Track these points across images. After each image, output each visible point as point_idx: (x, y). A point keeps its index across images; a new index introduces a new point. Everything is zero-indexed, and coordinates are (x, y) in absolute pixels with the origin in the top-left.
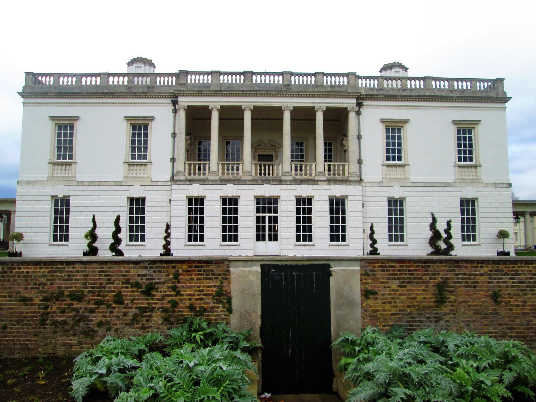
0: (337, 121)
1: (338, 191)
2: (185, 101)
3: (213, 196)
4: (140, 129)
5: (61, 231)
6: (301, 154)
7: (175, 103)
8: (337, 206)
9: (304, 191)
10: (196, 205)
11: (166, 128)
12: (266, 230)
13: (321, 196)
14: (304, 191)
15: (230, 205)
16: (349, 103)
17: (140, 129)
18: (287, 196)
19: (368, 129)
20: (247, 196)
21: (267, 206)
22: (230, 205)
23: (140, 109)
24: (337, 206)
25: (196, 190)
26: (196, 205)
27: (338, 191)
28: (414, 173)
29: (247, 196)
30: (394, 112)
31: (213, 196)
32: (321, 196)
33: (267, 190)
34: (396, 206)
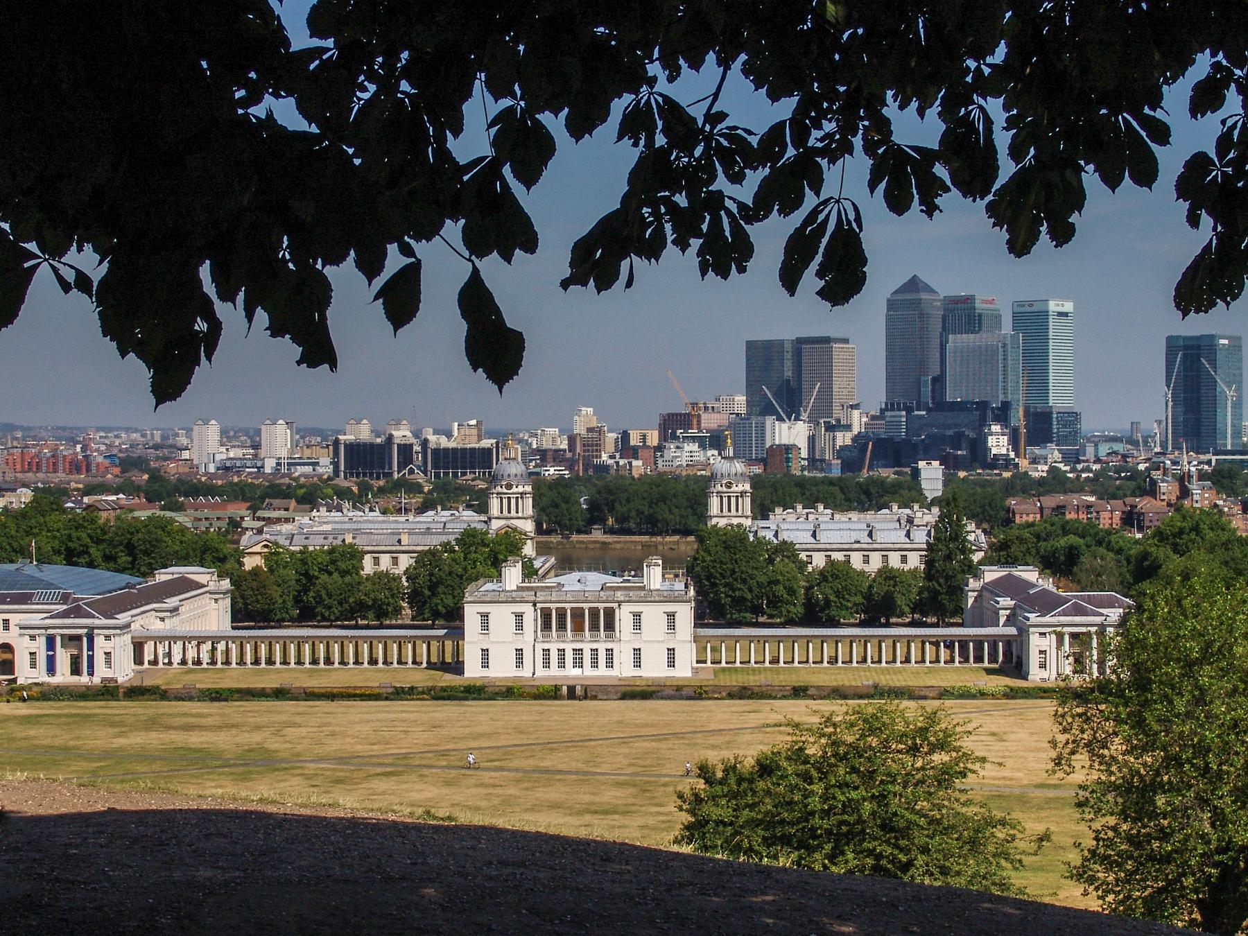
0: (610, 614)
1: (610, 646)
3: (554, 648)
4: (519, 616)
5: (485, 664)
6: (594, 627)
7: (535, 605)
8: (610, 652)
10: (546, 652)
12: (578, 663)
13: (602, 648)
15: (562, 652)
17: (519, 616)
18: (587, 648)
19: (624, 616)
20: (569, 648)
21: (578, 652)
22: (562, 652)
23: (518, 608)
24: (610, 652)
25: (546, 646)
26: (546, 652)
28: (645, 636)
29: (569, 648)
31: (554, 648)
32: (602, 648)
33: (578, 646)
34: (637, 651)
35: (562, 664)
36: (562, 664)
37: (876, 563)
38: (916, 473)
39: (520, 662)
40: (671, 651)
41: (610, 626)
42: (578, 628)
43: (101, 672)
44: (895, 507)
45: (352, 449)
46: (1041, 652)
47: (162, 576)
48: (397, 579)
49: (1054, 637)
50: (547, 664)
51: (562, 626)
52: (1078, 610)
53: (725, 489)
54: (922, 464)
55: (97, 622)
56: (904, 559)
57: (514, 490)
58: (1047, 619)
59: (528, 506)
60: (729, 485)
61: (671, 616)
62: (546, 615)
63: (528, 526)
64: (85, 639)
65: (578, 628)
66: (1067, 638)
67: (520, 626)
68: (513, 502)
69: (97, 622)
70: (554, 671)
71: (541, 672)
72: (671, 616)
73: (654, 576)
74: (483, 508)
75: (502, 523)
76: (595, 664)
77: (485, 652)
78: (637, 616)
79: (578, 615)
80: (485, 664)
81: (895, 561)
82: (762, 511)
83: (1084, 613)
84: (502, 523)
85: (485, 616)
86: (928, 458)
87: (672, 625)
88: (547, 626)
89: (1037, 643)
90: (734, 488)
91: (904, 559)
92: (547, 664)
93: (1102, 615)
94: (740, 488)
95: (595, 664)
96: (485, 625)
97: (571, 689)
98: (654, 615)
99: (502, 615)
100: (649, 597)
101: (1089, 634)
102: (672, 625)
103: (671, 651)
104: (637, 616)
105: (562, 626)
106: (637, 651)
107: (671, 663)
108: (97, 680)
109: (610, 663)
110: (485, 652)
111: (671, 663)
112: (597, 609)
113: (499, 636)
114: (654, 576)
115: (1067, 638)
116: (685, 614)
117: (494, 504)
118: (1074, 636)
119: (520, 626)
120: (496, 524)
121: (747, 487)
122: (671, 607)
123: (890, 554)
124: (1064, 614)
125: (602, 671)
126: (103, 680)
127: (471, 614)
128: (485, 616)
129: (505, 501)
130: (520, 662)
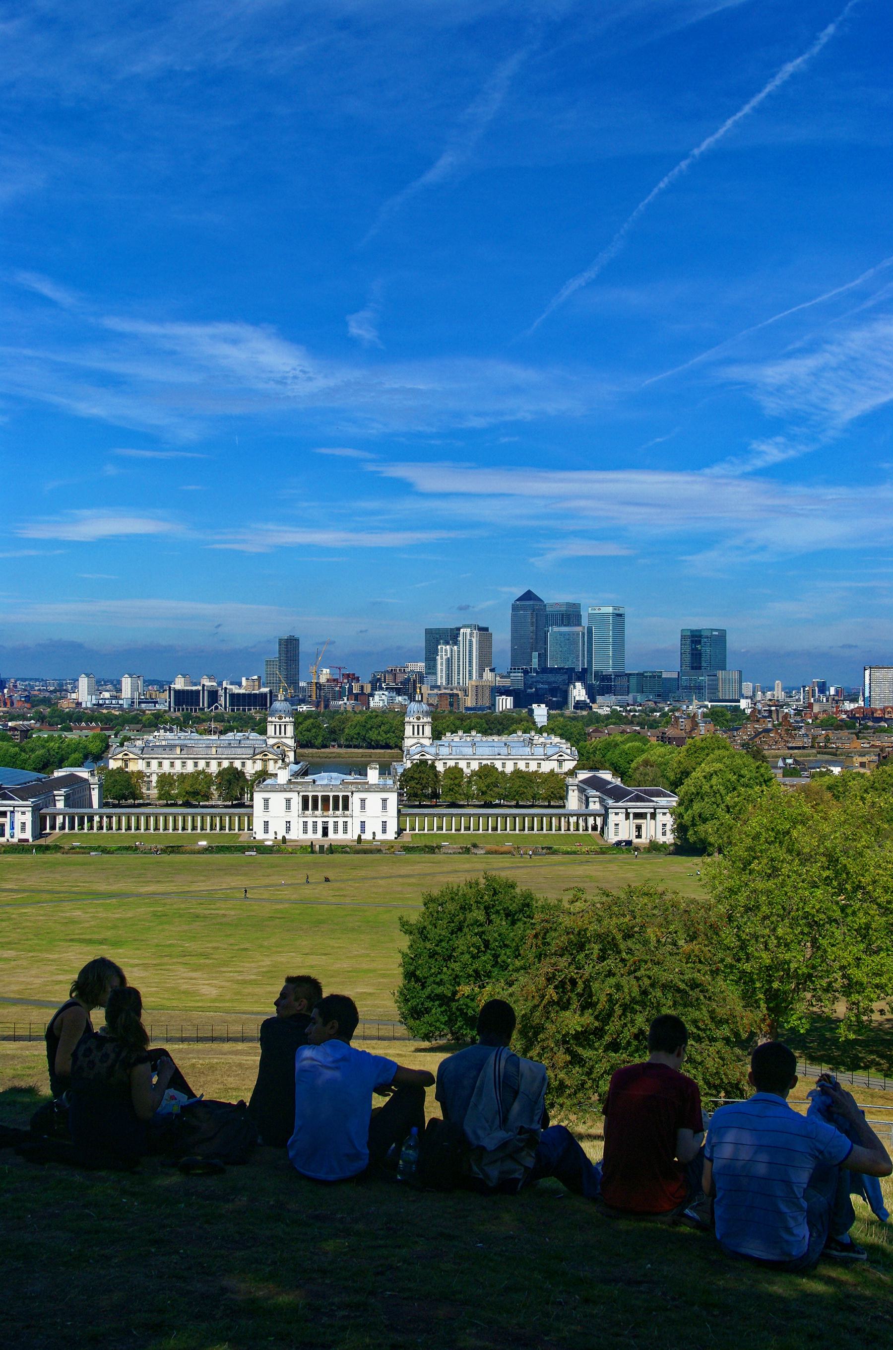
0: (346, 799)
1: (345, 819)
2: (301, 794)
3: (310, 821)
4: (288, 801)
5: (266, 831)
9: (336, 819)
10: (305, 823)
11: (296, 801)
13: (341, 821)
14: (336, 819)
16: (349, 794)
17: (288, 801)
18: (331, 821)
19: (355, 801)
20: (320, 821)
25: (305, 819)
26: (305, 823)
27: (345, 819)
30: (363, 795)
31: (310, 821)
32: (341, 821)
34: (363, 823)
35: (315, 831)
36: (315, 831)
37: (509, 768)
38: (531, 711)
39: (288, 829)
40: (384, 823)
41: (346, 807)
42: (326, 808)
43: (19, 835)
44: (520, 733)
45: (178, 693)
46: (617, 825)
47: (57, 774)
48: (208, 776)
49: (624, 815)
50: (305, 831)
51: (315, 807)
52: (638, 799)
53: (415, 720)
54: (534, 706)
55: (16, 803)
56: (527, 765)
57: (283, 720)
58: (620, 804)
59: (290, 730)
60: (418, 718)
61: (384, 801)
62: (305, 799)
63: (291, 742)
64: (8, 814)
65: (326, 808)
66: (631, 816)
67: (288, 807)
68: (283, 727)
69: (16, 803)
70: (310, 836)
71: (302, 836)
72: (384, 801)
73: (373, 776)
74: (264, 732)
75: (276, 741)
76: (336, 831)
77: (266, 823)
78: (363, 801)
79: (326, 799)
80: (266, 831)
81: (522, 766)
82: (437, 735)
83: (642, 800)
84: (276, 741)
85: (266, 801)
86: (539, 702)
87: (384, 807)
88: (305, 807)
89: (612, 819)
90: (421, 720)
91: (527, 765)
92: (305, 831)
93: (653, 801)
94: (425, 720)
95: (336, 831)
96: (266, 807)
97: (322, 847)
98: (374, 800)
99: (277, 800)
100: (369, 788)
101: (646, 813)
102: (384, 807)
103: (384, 823)
104: (363, 801)
105: (315, 807)
106: (363, 823)
107: (384, 831)
108: (15, 840)
109: (345, 831)
110: (266, 823)
111: (384, 831)
112: (338, 796)
113: (276, 815)
114: (373, 776)
115: (631, 816)
116: (393, 798)
117: (270, 729)
118: (637, 816)
119: (288, 807)
120: (271, 742)
121: (429, 720)
122: (384, 795)
123: (519, 762)
124: (630, 800)
125: (340, 836)
126: (20, 840)
127: (258, 797)
128: (266, 801)
129: (278, 727)
130: (288, 829)
